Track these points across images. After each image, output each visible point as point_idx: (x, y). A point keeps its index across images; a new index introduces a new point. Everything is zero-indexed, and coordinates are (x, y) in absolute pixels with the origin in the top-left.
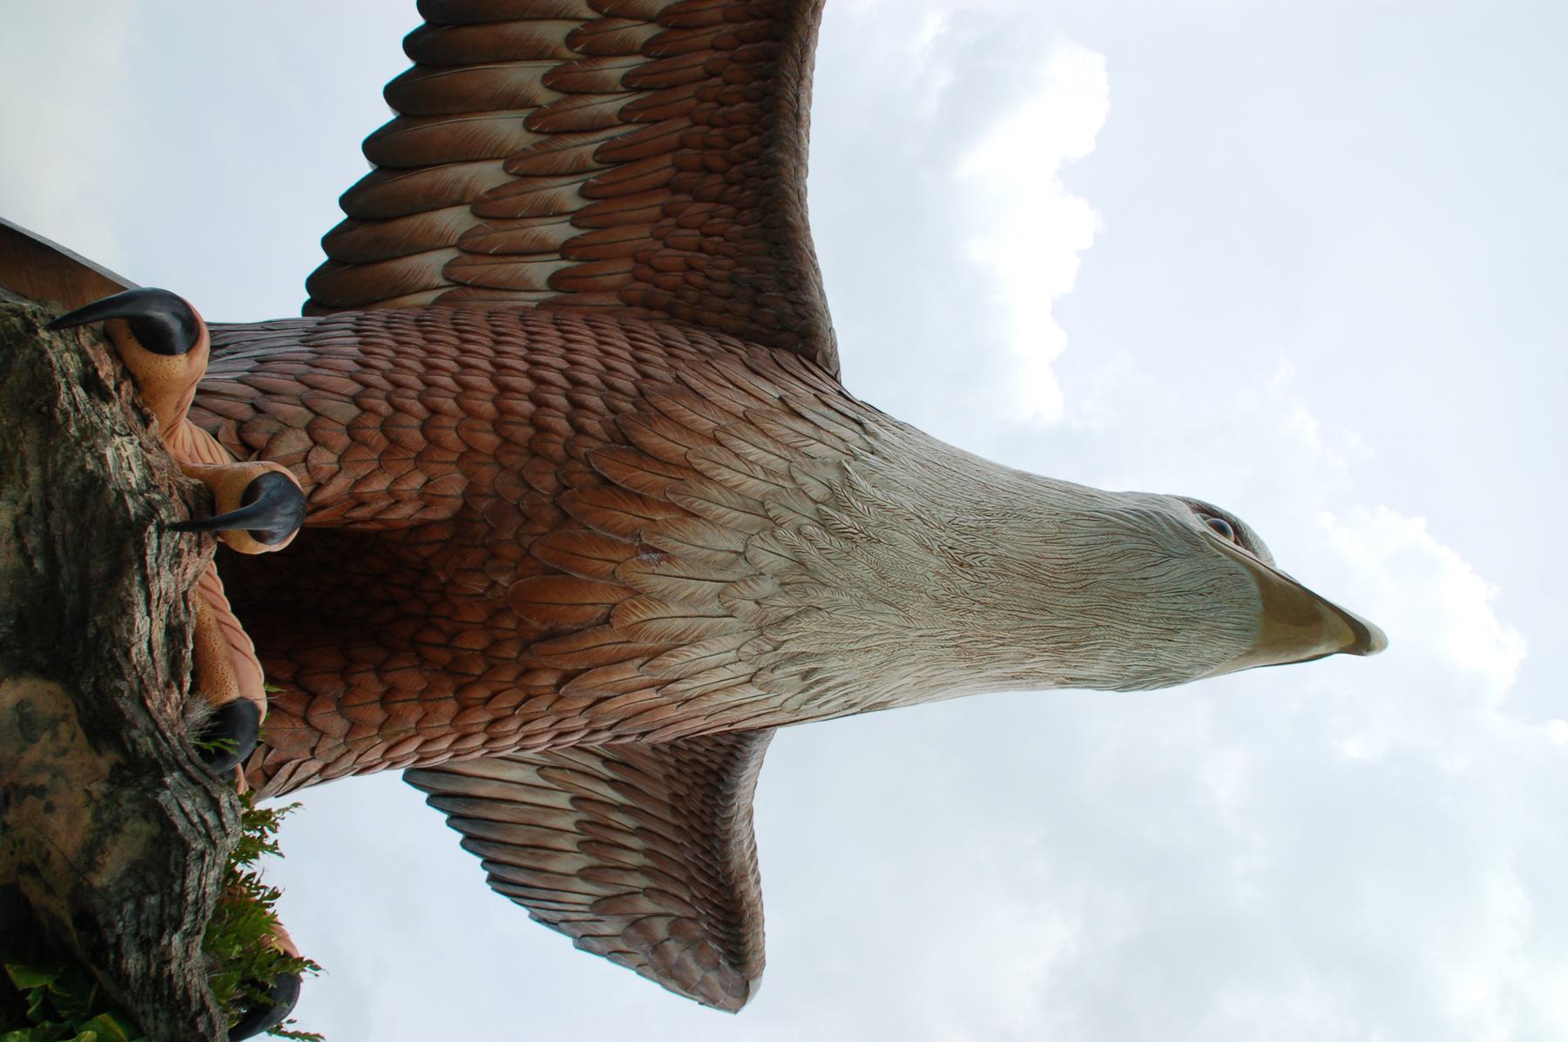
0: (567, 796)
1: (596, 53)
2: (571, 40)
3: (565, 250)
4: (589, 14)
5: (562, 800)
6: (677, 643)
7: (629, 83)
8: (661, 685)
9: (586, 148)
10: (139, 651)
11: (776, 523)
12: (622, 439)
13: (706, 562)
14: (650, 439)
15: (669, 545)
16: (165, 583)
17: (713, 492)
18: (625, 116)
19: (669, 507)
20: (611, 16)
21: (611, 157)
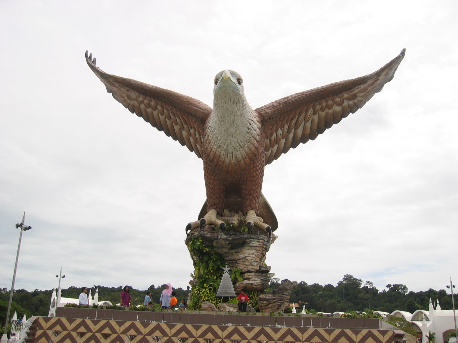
0: (314, 116)
1: (171, 117)
2: (169, 120)
3: (199, 134)
4: (164, 116)
5: (316, 117)
6: (236, 158)
7: (174, 115)
8: (244, 159)
9: (185, 126)
10: (210, 236)
11: (220, 146)
12: (212, 161)
13: (225, 155)
14: (212, 157)
15: (223, 159)
16: (205, 233)
17: (217, 152)
18: (179, 119)
19: (219, 158)
20: (164, 114)
21: (186, 123)
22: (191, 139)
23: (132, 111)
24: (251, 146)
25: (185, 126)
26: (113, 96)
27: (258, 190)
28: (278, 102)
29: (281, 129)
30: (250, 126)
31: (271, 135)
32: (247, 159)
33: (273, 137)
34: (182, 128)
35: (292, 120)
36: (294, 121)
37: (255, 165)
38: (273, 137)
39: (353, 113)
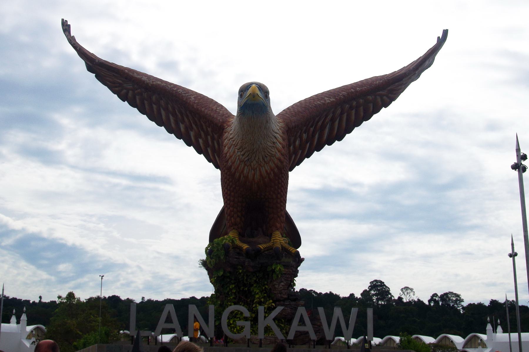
9: (194, 126)
22: (201, 141)
23: (123, 98)
24: (276, 161)
25: (194, 126)
26: (96, 76)
27: (282, 208)
28: (303, 106)
29: (305, 133)
30: (275, 140)
31: (295, 142)
32: (272, 176)
33: (297, 143)
34: (192, 129)
35: (318, 122)
36: (320, 123)
37: (280, 181)
38: (297, 143)
39: (385, 107)
